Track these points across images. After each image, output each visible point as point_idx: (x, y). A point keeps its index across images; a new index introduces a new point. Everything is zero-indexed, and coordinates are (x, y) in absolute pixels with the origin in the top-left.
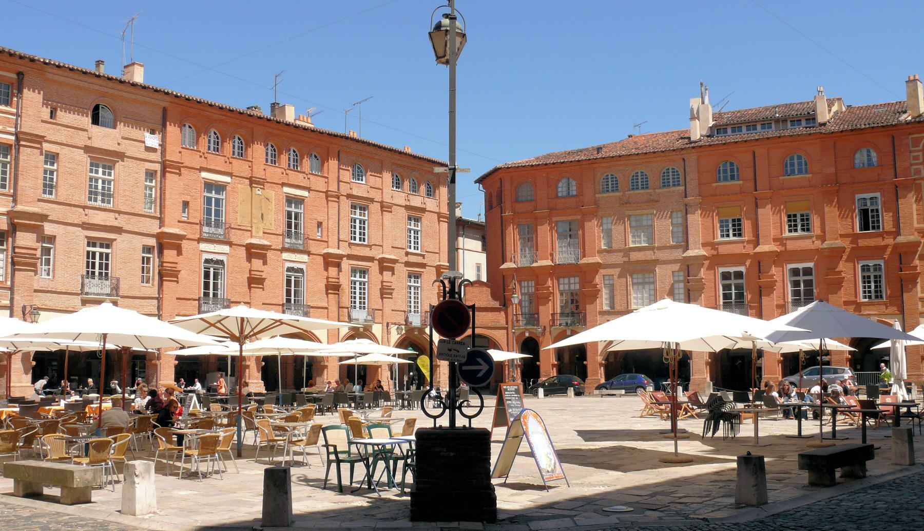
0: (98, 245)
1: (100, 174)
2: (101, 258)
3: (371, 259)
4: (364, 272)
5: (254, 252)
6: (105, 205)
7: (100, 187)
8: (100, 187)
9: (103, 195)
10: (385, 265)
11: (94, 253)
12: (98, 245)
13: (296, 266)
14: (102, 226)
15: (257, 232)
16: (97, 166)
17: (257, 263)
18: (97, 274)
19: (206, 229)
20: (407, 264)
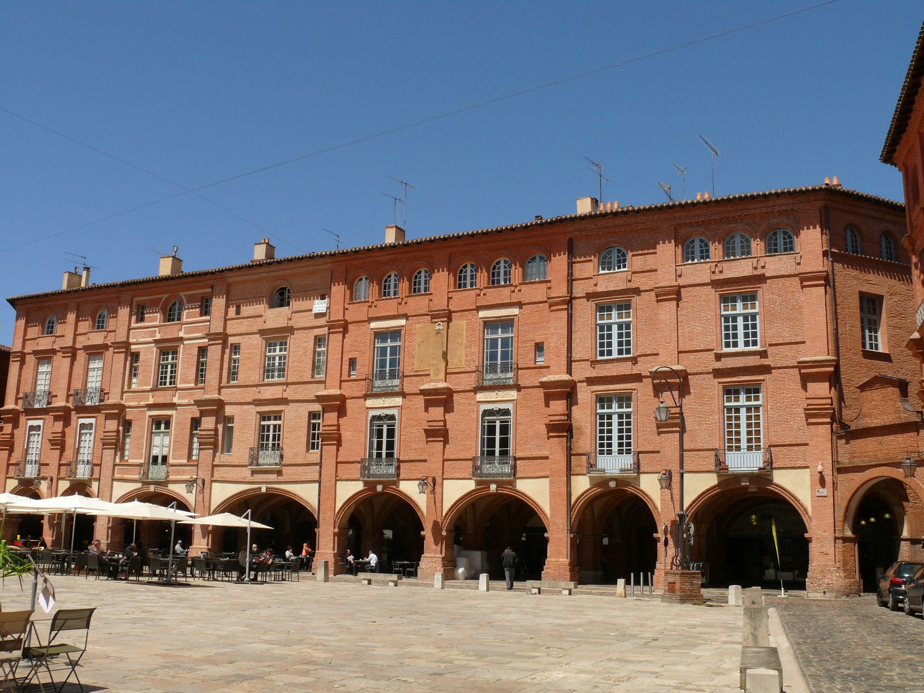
0: (272, 418)
1: (278, 352)
2: (274, 431)
3: (638, 378)
4: (625, 399)
5: (443, 399)
6: (282, 380)
7: (277, 364)
8: (277, 364)
9: (279, 370)
10: (676, 383)
11: (269, 426)
12: (272, 418)
13: (496, 407)
14: (272, 400)
15: (437, 375)
16: (275, 345)
17: (437, 412)
18: (270, 445)
19: (378, 383)
20: (718, 373)
